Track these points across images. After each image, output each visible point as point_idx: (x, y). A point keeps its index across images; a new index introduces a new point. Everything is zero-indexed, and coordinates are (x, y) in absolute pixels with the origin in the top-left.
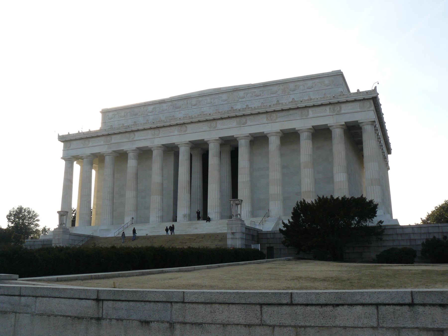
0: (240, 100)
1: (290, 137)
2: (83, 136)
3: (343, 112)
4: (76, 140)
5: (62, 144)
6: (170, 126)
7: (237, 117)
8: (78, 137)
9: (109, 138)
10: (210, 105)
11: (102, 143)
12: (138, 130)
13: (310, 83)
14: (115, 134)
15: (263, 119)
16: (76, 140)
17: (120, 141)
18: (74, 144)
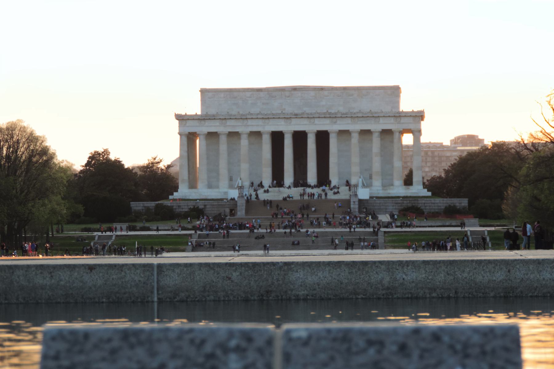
5: (177, 121)
9: (224, 121)
11: (218, 124)
12: (252, 118)
15: (349, 121)
18: (189, 123)
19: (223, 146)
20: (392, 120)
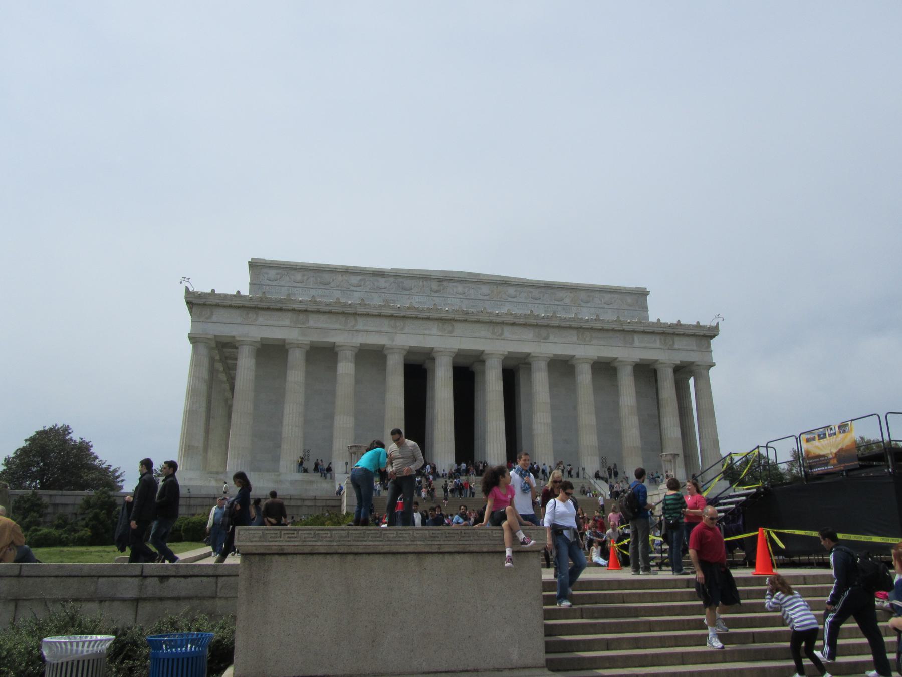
0: (510, 300)
1: (605, 370)
2: (247, 304)
3: (676, 346)
4: (230, 307)
6: (428, 319)
7: (537, 326)
8: (235, 302)
9: (302, 317)
10: (461, 296)
11: (287, 322)
12: (367, 315)
13: (608, 297)
14: (318, 312)
15: (573, 337)
16: (230, 307)
17: (325, 326)
18: (220, 315)
19: (296, 375)
20: (657, 342)
